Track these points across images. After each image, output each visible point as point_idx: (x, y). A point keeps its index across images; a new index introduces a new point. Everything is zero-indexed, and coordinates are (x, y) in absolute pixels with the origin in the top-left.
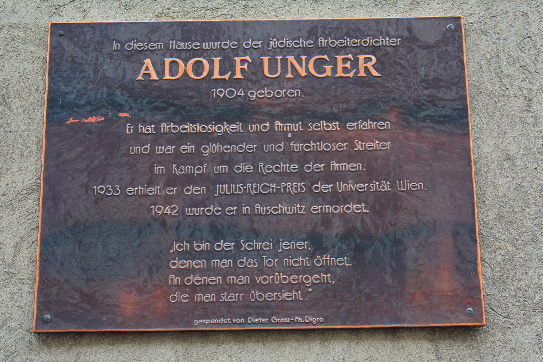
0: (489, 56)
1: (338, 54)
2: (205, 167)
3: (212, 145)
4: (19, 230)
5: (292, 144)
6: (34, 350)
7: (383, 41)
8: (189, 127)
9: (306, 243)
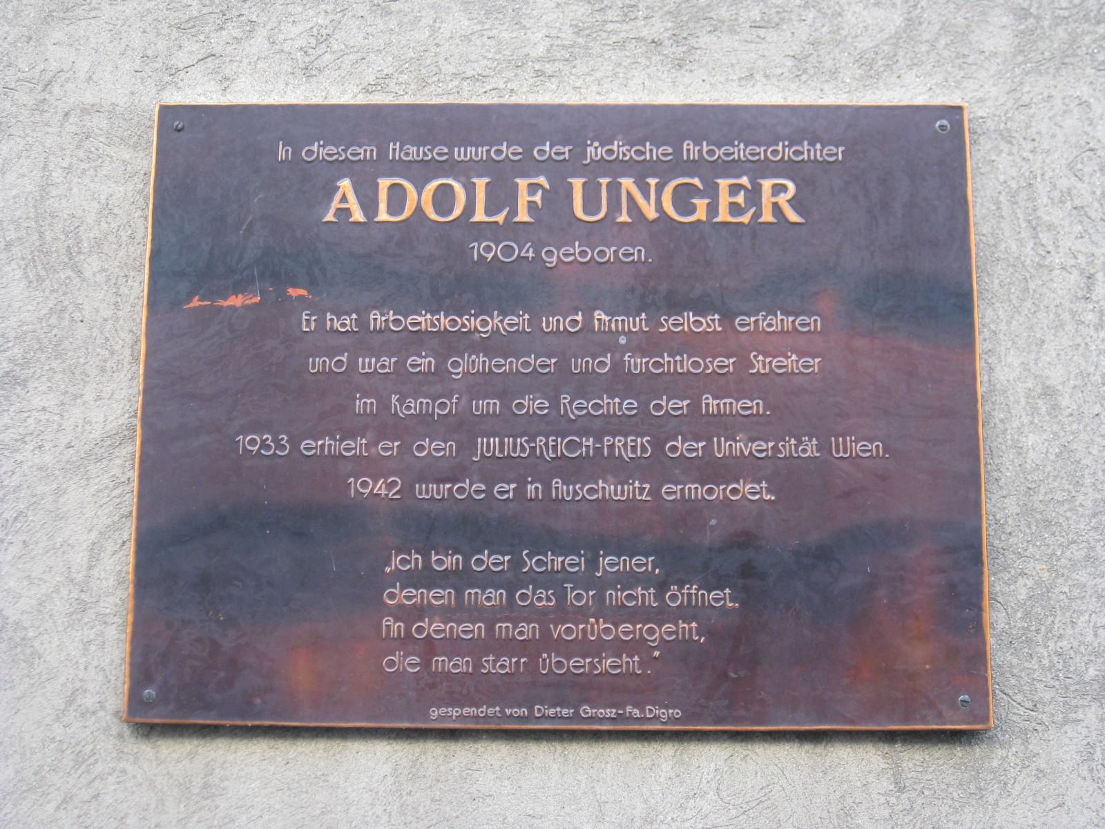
0: (1014, 185)
1: (764, 177)
2: (454, 401)
3: (469, 357)
4: (98, 517)
5: (626, 358)
6: (128, 753)
7: (810, 152)
8: (424, 320)
9: (650, 559)
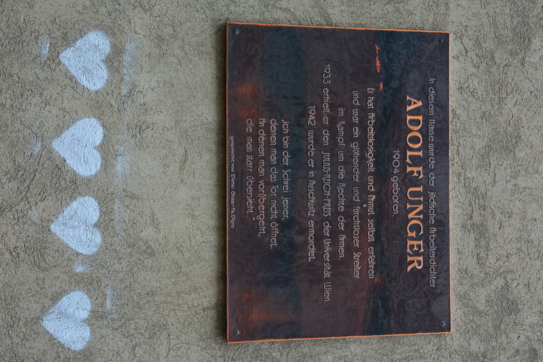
0: (421, 351)
7: (433, 274)
8: (371, 133)
